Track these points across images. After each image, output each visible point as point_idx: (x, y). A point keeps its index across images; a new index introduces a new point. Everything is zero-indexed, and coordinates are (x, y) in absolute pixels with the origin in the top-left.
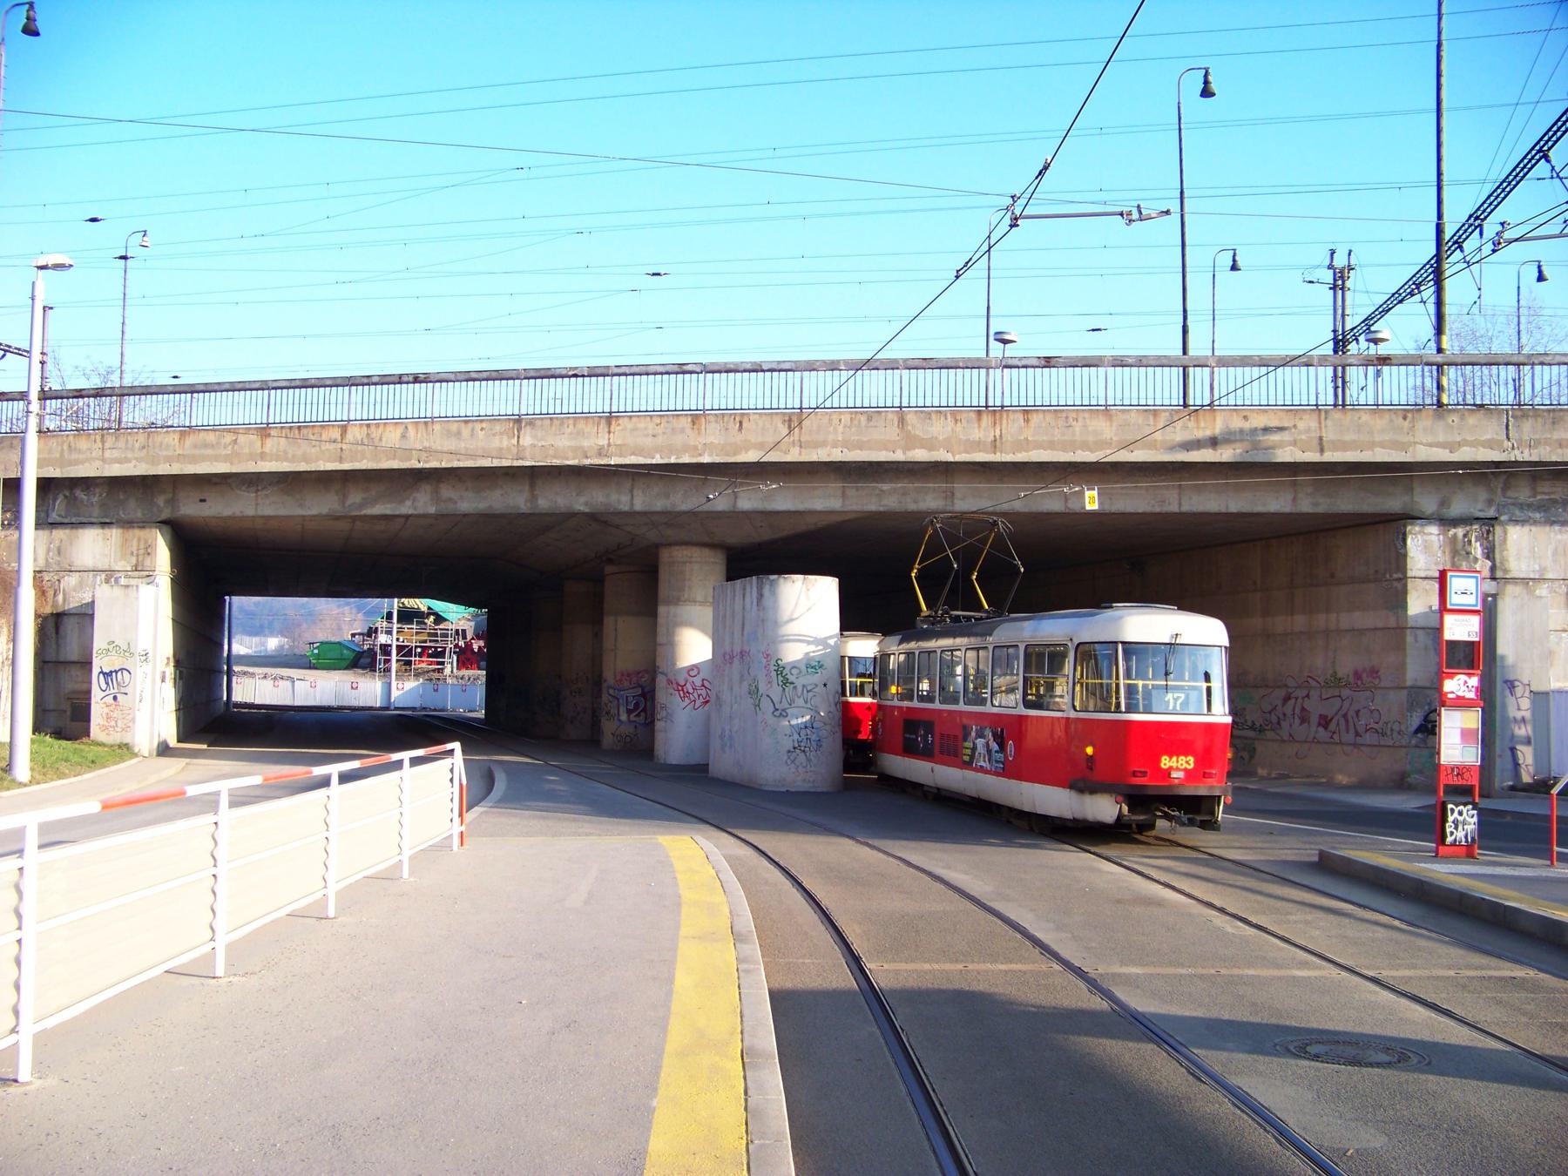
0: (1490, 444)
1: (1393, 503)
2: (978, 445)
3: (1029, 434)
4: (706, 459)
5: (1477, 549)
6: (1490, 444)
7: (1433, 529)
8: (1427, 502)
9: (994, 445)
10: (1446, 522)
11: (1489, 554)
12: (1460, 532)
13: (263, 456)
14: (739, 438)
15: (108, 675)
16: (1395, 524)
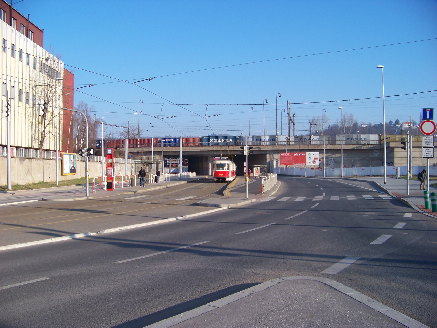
0: (272, 148)
1: (265, 153)
2: (232, 149)
3: (236, 148)
4: (211, 150)
5: (272, 156)
6: (272, 148)
7: (269, 155)
8: (268, 152)
9: (233, 149)
10: (270, 154)
11: (273, 157)
12: (271, 155)
13: (173, 150)
14: (213, 148)
15: (160, 169)
16: (265, 155)
